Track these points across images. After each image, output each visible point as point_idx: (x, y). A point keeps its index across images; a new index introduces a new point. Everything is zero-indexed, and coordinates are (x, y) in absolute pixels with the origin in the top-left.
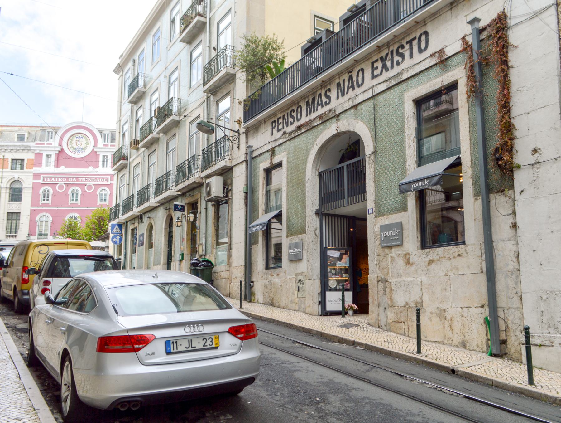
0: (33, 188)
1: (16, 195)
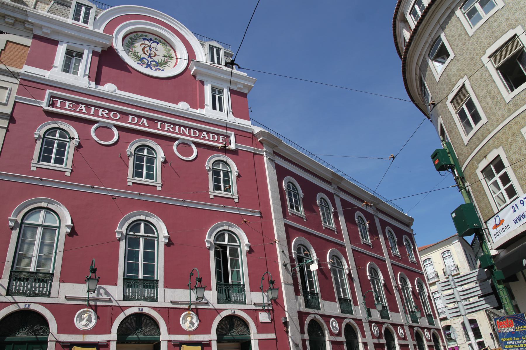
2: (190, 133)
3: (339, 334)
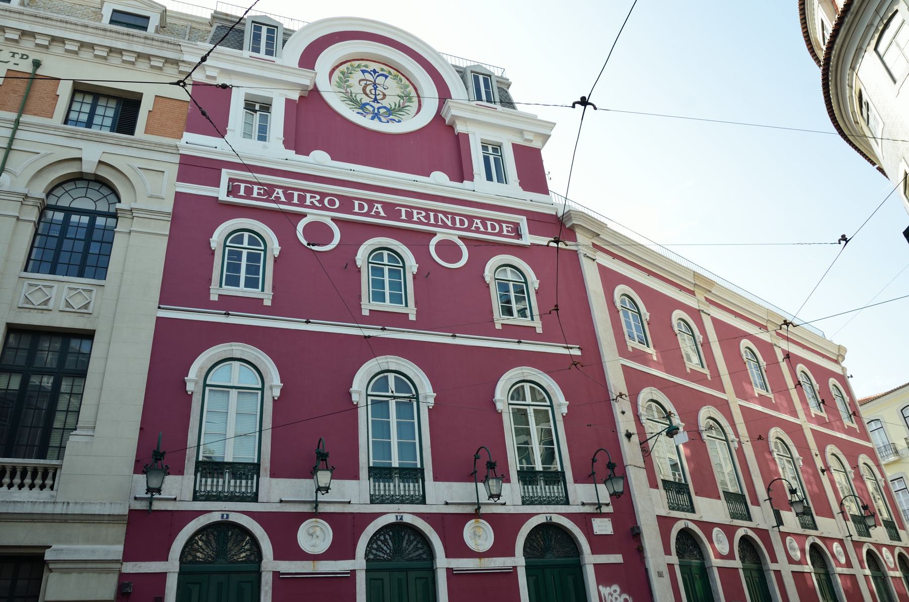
0: (176, 218)
1: (71, 240)
3: (731, 556)
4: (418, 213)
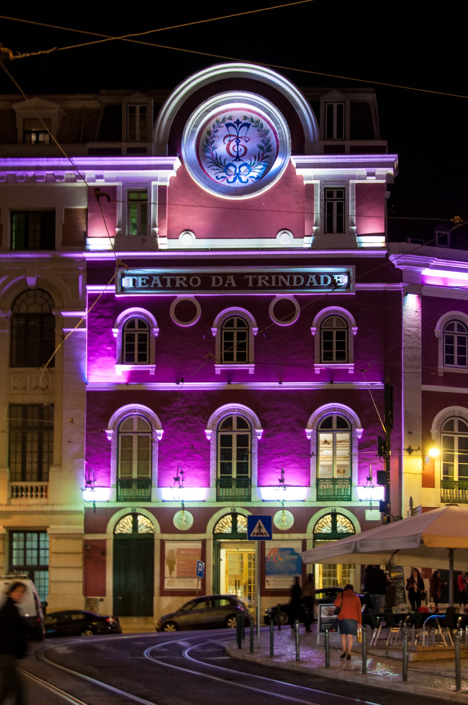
2: (291, 282)
4: (263, 278)
